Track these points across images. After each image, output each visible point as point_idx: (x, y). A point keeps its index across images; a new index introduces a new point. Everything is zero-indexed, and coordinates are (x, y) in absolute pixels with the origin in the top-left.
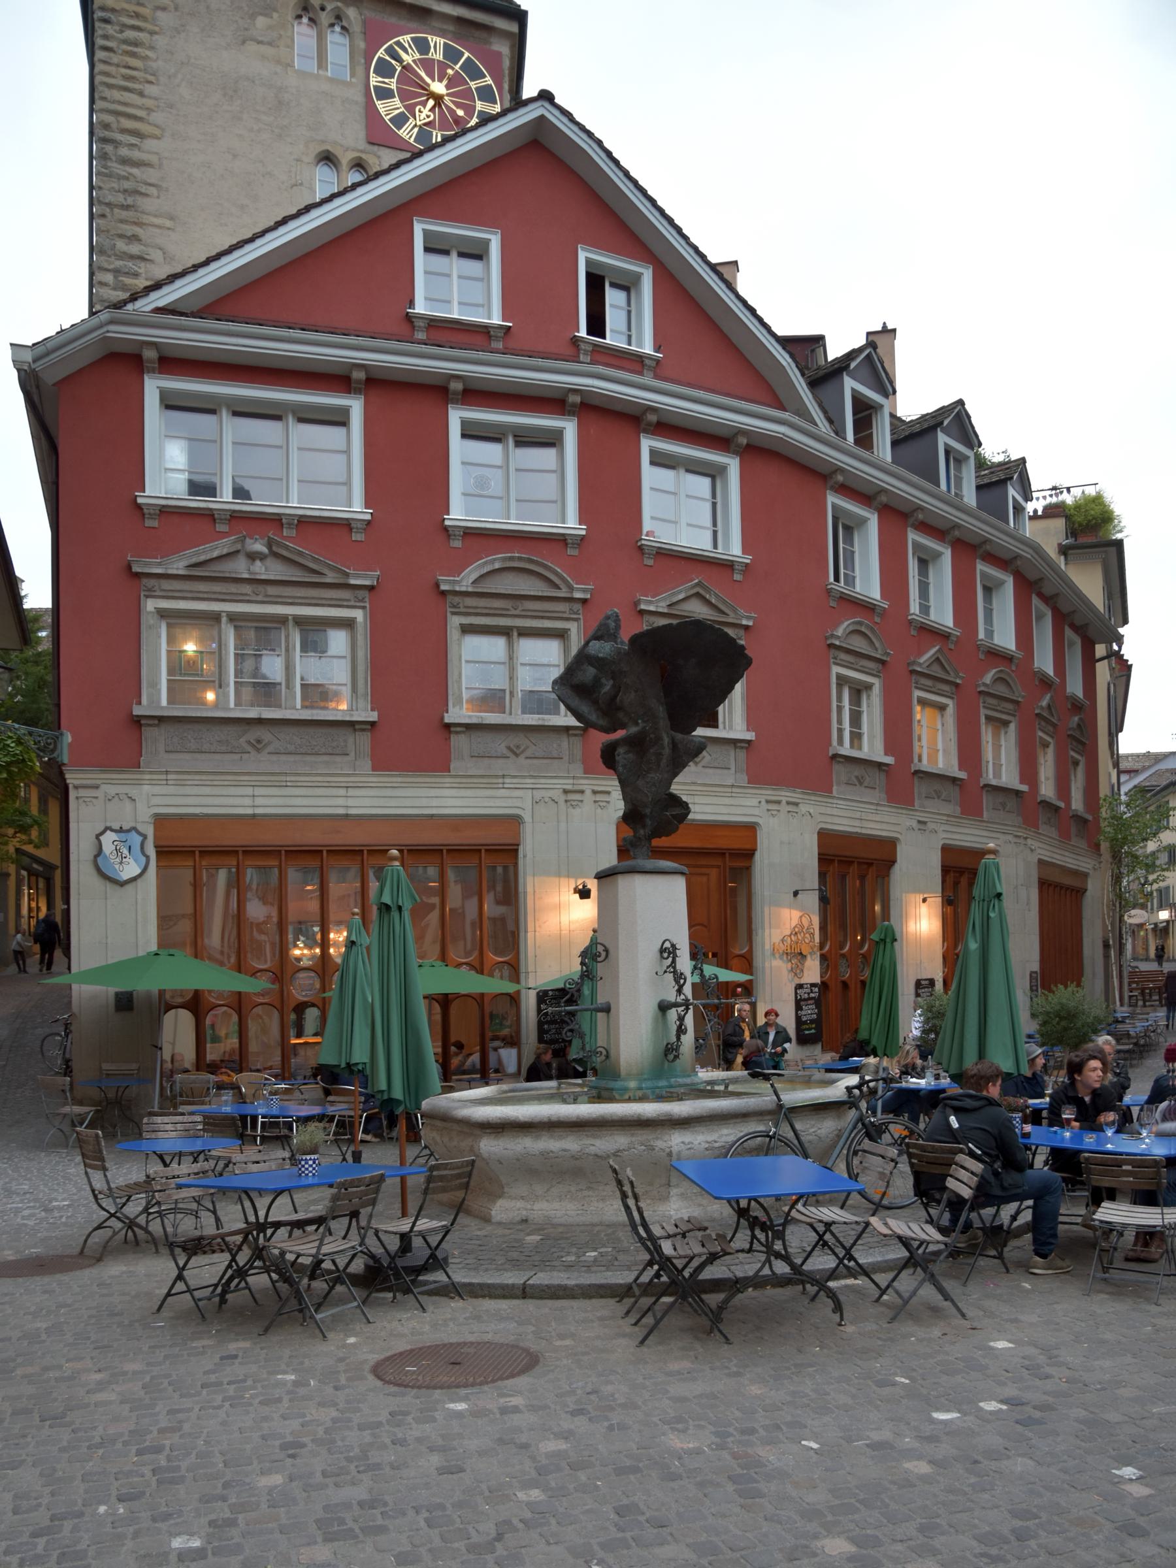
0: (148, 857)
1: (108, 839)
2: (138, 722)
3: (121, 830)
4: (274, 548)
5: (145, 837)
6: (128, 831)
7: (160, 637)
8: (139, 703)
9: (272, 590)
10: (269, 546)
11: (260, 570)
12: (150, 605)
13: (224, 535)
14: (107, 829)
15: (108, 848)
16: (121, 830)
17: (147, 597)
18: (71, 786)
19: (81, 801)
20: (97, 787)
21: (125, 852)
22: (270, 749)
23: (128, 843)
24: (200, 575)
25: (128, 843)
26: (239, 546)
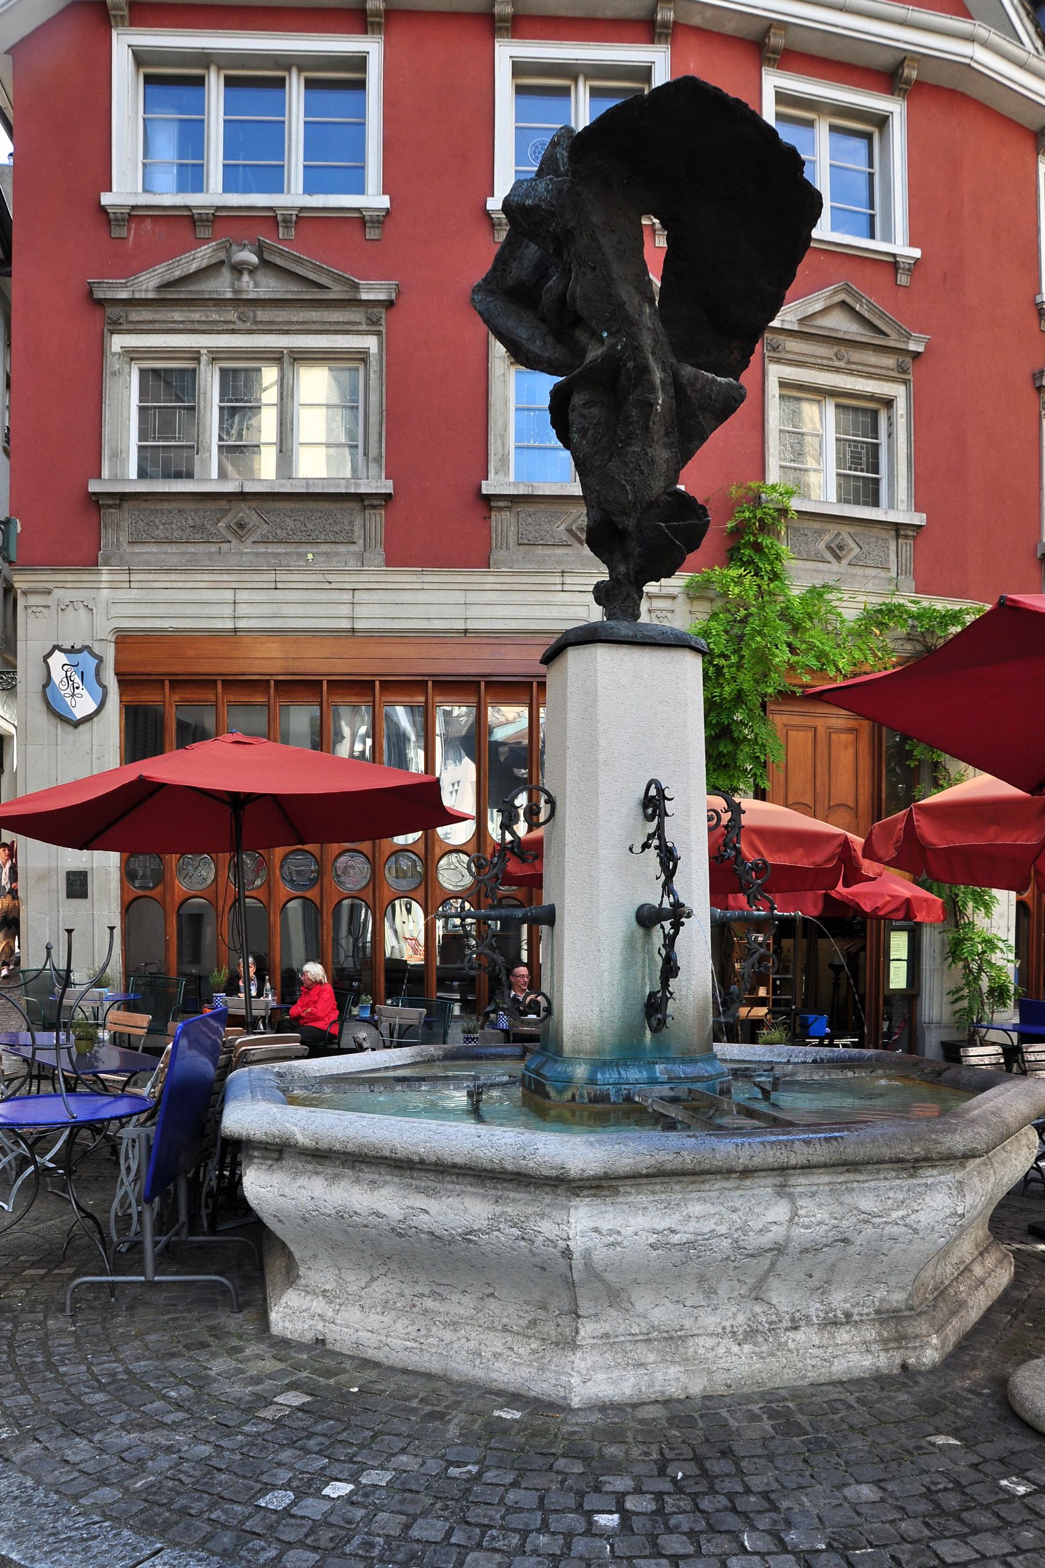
0: (104, 687)
1: (58, 660)
2: (98, 502)
3: (72, 651)
4: (266, 256)
5: (100, 659)
6: (80, 651)
7: (129, 387)
8: (99, 476)
9: (262, 315)
10: (259, 253)
11: (249, 287)
12: (118, 342)
13: (206, 241)
14: (56, 647)
15: (57, 675)
16: (72, 651)
17: (112, 332)
18: (19, 591)
19: (30, 611)
20: (49, 592)
21: (77, 680)
22: (256, 536)
23: (80, 669)
24: (176, 298)
25: (80, 669)
26: (222, 255)
